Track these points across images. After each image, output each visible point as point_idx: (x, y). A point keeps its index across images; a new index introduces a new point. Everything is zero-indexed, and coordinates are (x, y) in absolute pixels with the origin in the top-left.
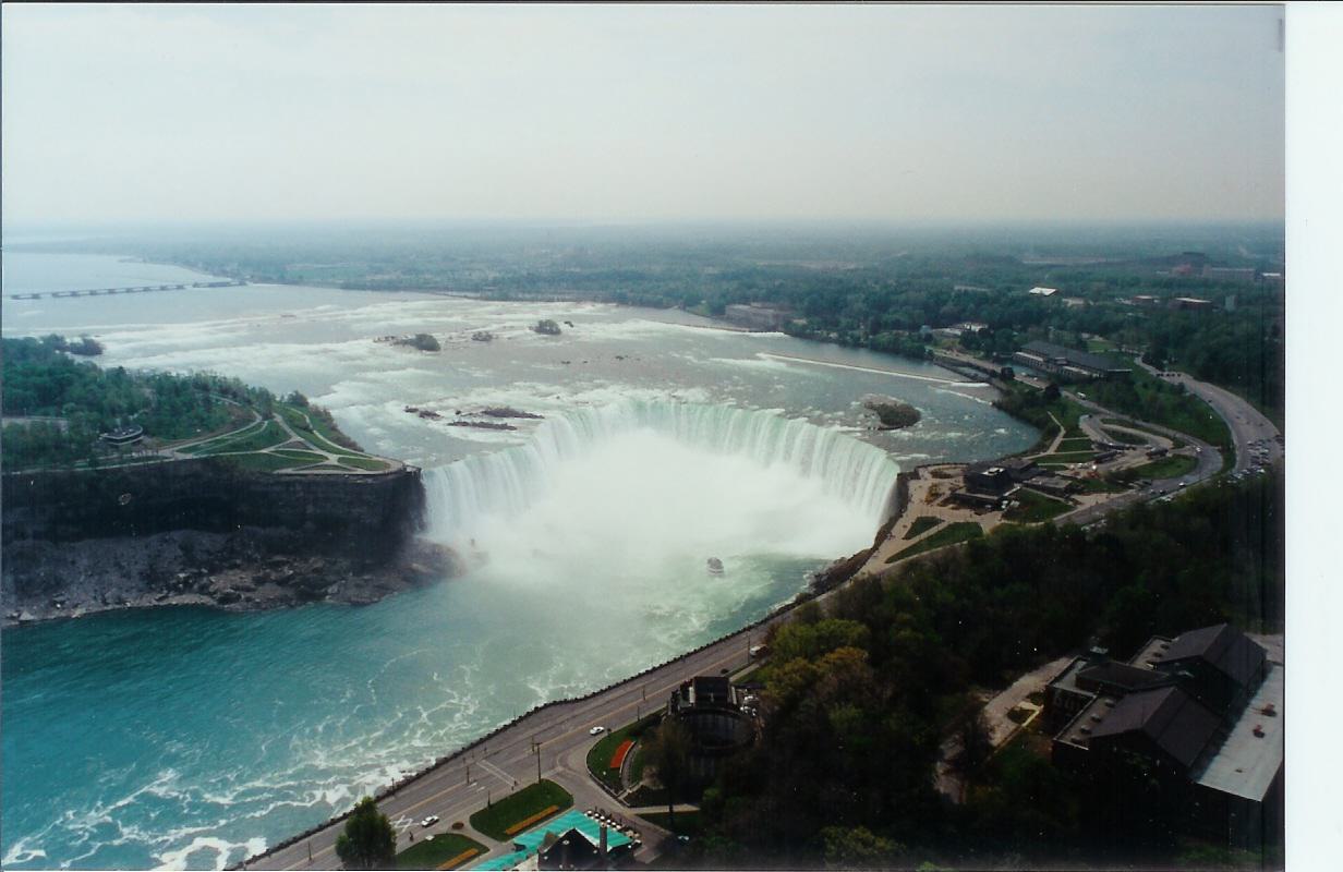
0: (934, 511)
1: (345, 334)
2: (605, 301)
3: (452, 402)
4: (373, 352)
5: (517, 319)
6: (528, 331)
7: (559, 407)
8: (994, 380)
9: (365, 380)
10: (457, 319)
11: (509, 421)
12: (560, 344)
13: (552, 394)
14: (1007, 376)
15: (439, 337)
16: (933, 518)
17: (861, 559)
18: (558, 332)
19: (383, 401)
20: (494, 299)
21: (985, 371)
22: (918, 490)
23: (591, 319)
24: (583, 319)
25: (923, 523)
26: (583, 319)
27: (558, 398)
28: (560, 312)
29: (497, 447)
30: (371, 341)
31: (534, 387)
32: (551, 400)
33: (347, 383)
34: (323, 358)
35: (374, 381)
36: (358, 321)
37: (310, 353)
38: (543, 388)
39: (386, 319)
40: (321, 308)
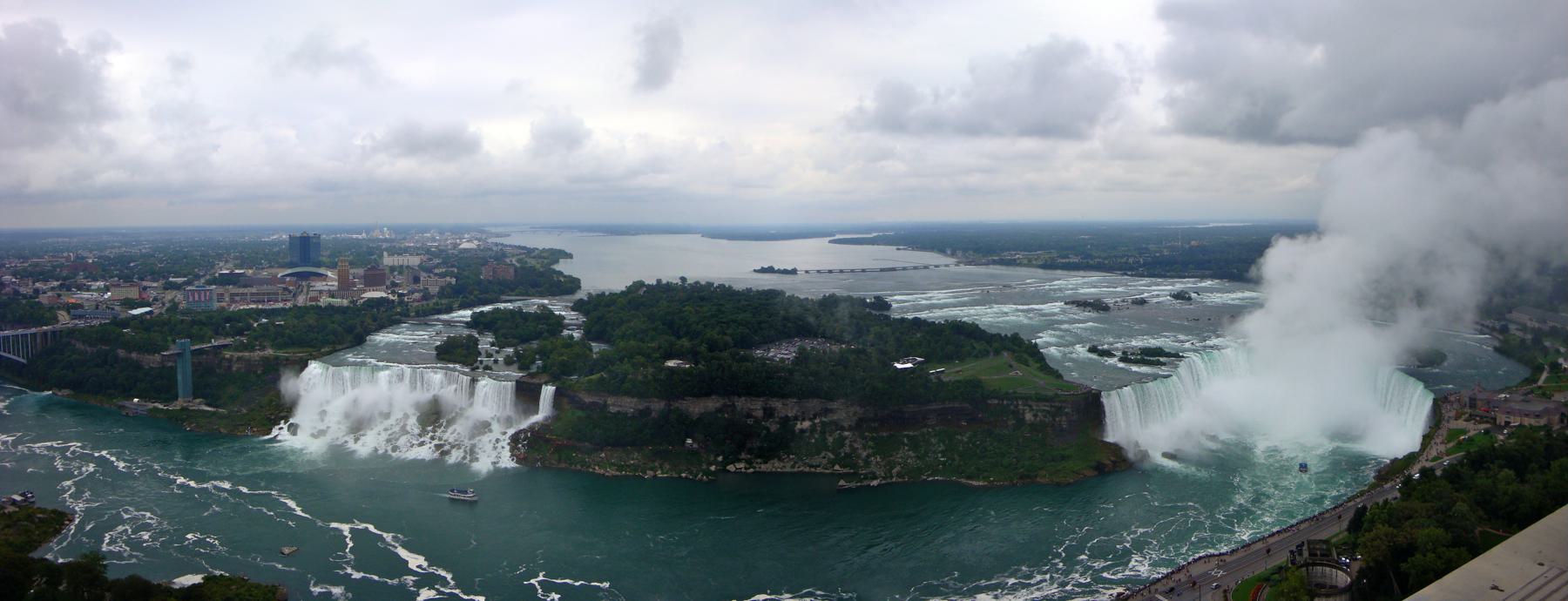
0: (1461, 424)
1: (1046, 298)
2: (1221, 277)
3: (1119, 345)
4: (1063, 311)
5: (1160, 291)
6: (1169, 297)
7: (1195, 351)
8: (1495, 334)
9: (1061, 330)
10: (1119, 289)
11: (1161, 359)
12: (1191, 307)
13: (1188, 341)
14: (1504, 330)
15: (1109, 301)
16: (1461, 429)
17: (1411, 458)
18: (1190, 299)
19: (1073, 344)
20: (1142, 276)
21: (1487, 327)
22: (1449, 411)
23: (1211, 290)
24: (1207, 290)
25: (1453, 434)
26: (1207, 290)
27: (1192, 344)
28: (1189, 285)
29: (1155, 377)
30: (1063, 303)
31: (1175, 336)
32: (1187, 345)
33: (1050, 332)
34: (1031, 315)
35: (1066, 330)
36: (1055, 290)
37: (1022, 311)
38: (1182, 337)
39: (1072, 289)
40: (1028, 281)
